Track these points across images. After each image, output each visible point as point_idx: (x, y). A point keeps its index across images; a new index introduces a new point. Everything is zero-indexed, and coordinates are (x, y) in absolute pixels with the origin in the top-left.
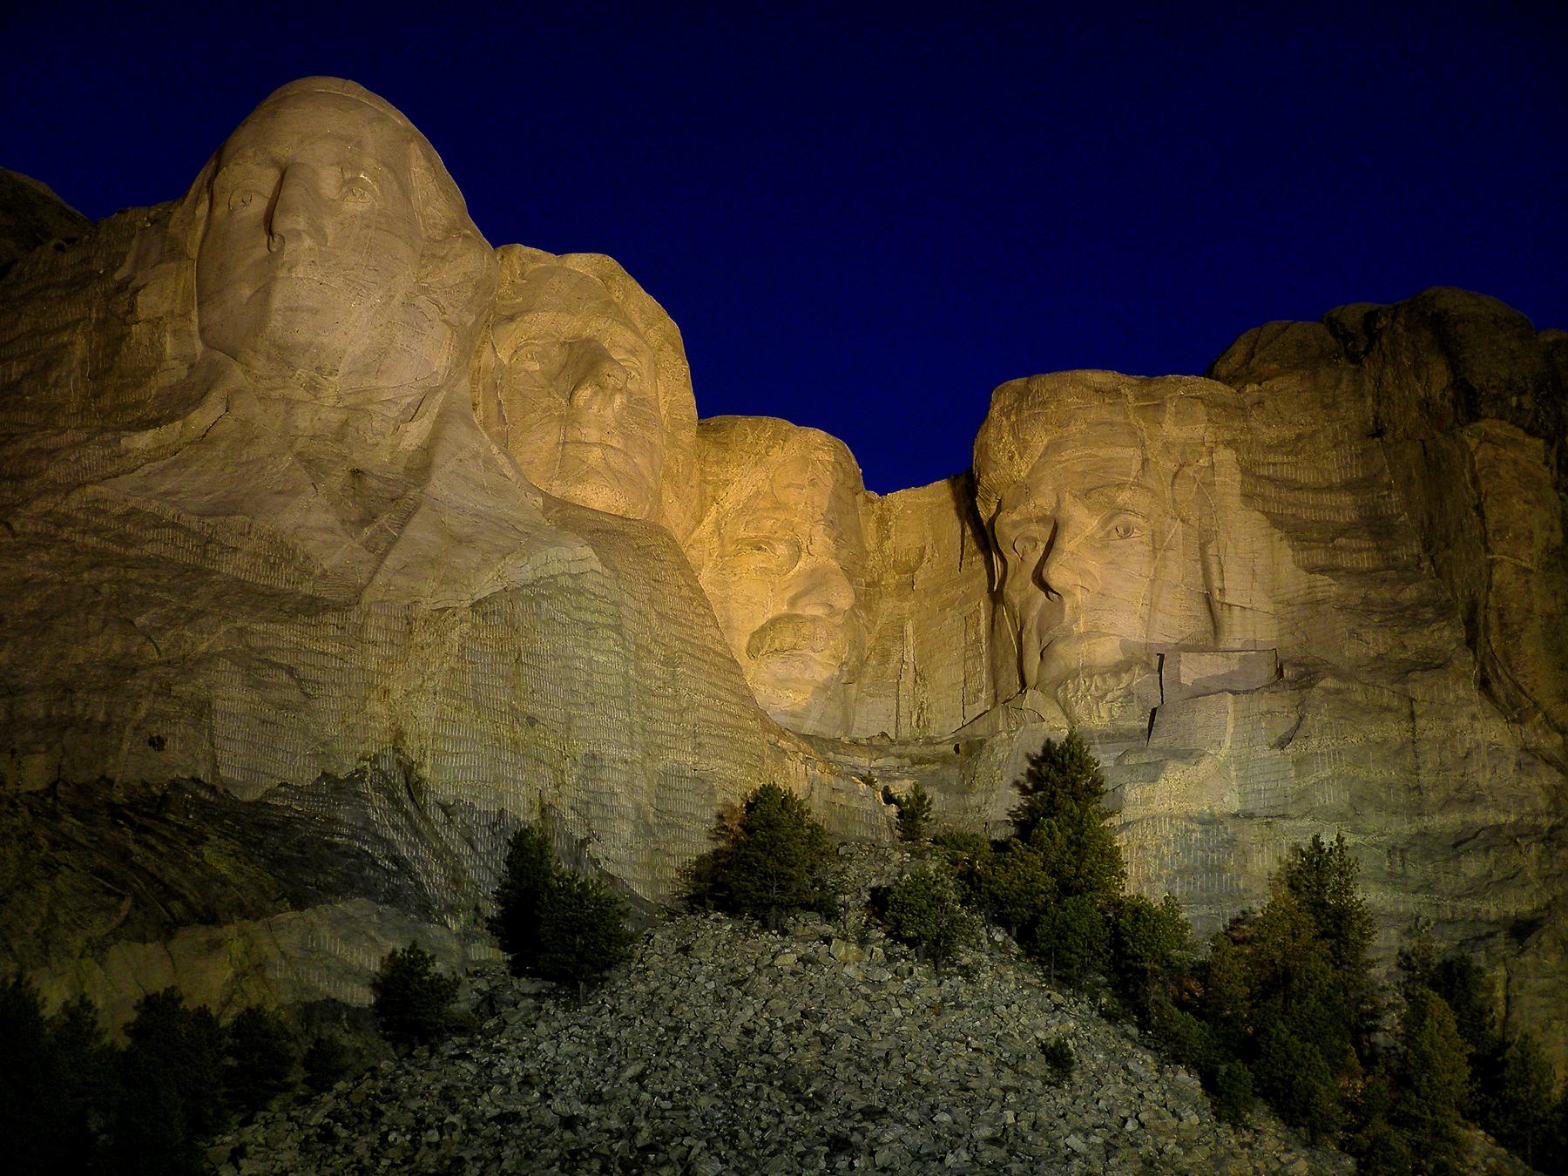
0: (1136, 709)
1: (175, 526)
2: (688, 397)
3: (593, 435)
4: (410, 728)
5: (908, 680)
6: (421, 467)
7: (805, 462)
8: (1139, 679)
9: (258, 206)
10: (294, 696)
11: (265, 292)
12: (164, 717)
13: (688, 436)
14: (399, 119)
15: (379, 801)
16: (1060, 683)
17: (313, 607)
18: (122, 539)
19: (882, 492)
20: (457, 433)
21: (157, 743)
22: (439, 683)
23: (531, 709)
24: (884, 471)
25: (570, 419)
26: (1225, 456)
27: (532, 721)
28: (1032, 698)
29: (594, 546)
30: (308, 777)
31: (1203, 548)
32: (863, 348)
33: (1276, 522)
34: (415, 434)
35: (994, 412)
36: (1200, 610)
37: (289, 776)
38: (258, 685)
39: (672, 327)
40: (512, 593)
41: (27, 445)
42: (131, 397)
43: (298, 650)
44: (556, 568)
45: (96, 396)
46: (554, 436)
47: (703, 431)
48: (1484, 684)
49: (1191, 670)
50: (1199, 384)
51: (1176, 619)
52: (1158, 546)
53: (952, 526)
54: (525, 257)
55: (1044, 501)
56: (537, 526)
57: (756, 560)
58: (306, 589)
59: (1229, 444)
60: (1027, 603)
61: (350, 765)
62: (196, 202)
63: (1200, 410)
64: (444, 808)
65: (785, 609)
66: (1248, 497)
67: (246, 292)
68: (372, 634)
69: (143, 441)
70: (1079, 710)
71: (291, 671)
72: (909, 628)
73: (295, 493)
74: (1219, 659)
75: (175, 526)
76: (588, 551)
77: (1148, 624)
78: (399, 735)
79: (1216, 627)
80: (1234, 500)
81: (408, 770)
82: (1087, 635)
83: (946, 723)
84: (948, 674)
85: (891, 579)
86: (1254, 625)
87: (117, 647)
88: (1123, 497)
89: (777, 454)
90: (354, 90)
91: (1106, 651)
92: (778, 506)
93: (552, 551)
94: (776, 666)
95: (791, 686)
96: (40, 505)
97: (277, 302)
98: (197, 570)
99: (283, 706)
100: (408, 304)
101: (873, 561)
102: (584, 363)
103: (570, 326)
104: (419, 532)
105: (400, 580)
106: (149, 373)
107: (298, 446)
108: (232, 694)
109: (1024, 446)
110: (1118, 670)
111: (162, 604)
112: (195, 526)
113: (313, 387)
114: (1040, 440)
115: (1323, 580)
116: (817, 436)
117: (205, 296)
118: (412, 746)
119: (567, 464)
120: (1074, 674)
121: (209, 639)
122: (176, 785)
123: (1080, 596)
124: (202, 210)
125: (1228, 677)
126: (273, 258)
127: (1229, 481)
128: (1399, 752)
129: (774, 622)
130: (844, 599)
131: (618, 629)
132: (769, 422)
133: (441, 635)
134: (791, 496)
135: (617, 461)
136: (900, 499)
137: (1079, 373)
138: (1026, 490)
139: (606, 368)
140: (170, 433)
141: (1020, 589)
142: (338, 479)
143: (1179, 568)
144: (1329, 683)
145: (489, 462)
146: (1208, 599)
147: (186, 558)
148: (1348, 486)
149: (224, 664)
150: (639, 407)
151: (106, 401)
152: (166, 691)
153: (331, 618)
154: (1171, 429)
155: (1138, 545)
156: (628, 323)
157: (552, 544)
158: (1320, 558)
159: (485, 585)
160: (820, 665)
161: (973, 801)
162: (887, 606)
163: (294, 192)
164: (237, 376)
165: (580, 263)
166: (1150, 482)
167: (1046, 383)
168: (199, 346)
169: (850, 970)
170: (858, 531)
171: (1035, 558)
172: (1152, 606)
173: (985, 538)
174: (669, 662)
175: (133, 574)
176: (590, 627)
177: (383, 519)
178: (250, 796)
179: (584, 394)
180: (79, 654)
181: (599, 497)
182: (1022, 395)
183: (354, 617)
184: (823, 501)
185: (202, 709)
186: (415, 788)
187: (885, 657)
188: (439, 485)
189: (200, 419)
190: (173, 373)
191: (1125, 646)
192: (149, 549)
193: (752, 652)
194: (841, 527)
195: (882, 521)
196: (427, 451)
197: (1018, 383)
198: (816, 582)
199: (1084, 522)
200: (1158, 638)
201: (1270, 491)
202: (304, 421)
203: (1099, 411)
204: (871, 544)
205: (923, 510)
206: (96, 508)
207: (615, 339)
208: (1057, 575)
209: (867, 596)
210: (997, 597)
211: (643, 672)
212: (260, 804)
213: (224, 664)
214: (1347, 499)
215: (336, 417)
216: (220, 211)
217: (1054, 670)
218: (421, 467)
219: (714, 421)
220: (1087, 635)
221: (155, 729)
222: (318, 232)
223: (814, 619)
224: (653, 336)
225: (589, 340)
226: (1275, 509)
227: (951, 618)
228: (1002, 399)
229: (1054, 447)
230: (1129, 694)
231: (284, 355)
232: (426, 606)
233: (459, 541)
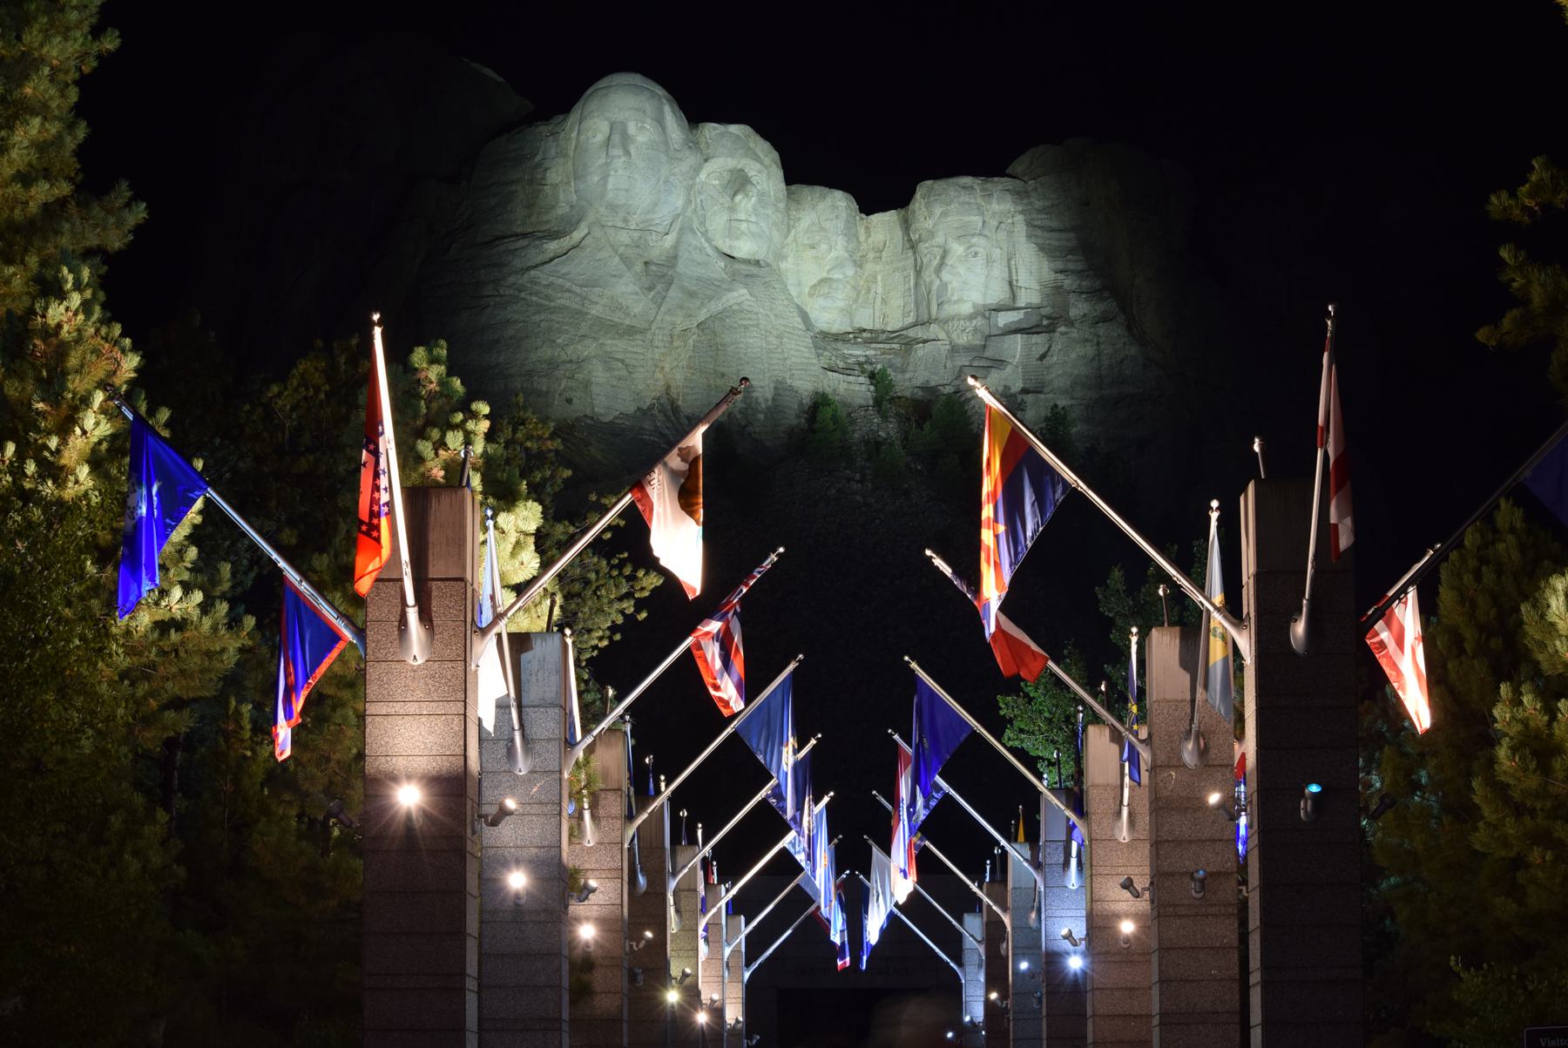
0: (979, 336)
1: (569, 291)
2: (779, 174)
3: (742, 216)
4: (673, 384)
5: (879, 301)
6: (673, 259)
7: (834, 207)
8: (979, 322)
9: (600, 138)
10: (625, 373)
11: (605, 178)
12: (571, 389)
13: (782, 205)
14: (660, 91)
15: (660, 417)
16: (946, 322)
17: (631, 331)
18: (547, 297)
19: (868, 214)
20: (689, 238)
21: (569, 401)
22: (685, 363)
23: (722, 370)
24: (869, 205)
25: (732, 209)
26: (1020, 218)
27: (723, 375)
28: (934, 328)
29: (746, 285)
30: (632, 409)
31: (1009, 260)
32: (861, 153)
33: (1042, 248)
34: (669, 240)
35: (918, 195)
36: (1007, 288)
37: (623, 410)
38: (611, 369)
39: (776, 155)
40: (713, 318)
41: (502, 248)
42: (545, 218)
43: (625, 351)
44: (732, 302)
45: (529, 216)
46: (725, 218)
47: (789, 194)
48: (1129, 328)
49: (1004, 319)
50: (1006, 182)
51: (998, 294)
52: (989, 261)
53: (899, 233)
54: (711, 130)
55: (939, 239)
56: (722, 281)
57: (810, 253)
58: (627, 322)
59: (1021, 212)
60: (931, 283)
61: (648, 402)
62: (571, 130)
63: (1008, 196)
64: (688, 418)
65: (825, 275)
66: (1029, 237)
67: (596, 178)
68: (656, 343)
69: (553, 246)
70: (954, 336)
71: (622, 361)
72: (879, 278)
73: (620, 277)
74: (1014, 313)
75: (569, 291)
76: (744, 291)
77: (985, 295)
78: (668, 387)
79: (1014, 297)
80: (1023, 239)
81: (672, 402)
82: (956, 302)
83: (894, 324)
84: (897, 302)
85: (871, 255)
86: (1030, 295)
87: (549, 352)
88: (975, 240)
89: (821, 206)
90: (637, 79)
91: (966, 309)
92: (823, 229)
93: (731, 295)
94: (821, 302)
95: (829, 315)
96: (511, 280)
97: (610, 186)
98: (579, 312)
99: (620, 379)
100: (666, 182)
101: (864, 246)
102: (739, 183)
103: (732, 163)
104: (673, 293)
105: (668, 318)
106: (553, 207)
107: (621, 250)
108: (598, 374)
109: (931, 214)
110: (971, 317)
111: (567, 332)
112: (578, 290)
113: (626, 220)
114: (938, 211)
115: (1061, 276)
116: (839, 194)
117: (577, 176)
118: (674, 392)
119: (731, 232)
120: (952, 318)
121: (588, 349)
122: (577, 419)
123: (955, 284)
124: (574, 135)
125: (1019, 321)
126: (607, 164)
127: (1021, 229)
128: (1093, 359)
129: (823, 281)
130: (850, 271)
131: (757, 326)
132: (819, 190)
133: (686, 342)
134: (827, 225)
135: (753, 228)
136: (877, 218)
137: (955, 180)
138: (932, 234)
139: (749, 187)
140: (565, 243)
141: (928, 275)
142: (639, 267)
143: (999, 271)
144: (1062, 329)
145: (701, 250)
146: (1010, 283)
147: (575, 306)
148: (1073, 229)
149: (595, 361)
150: (762, 195)
151: (534, 218)
152: (572, 378)
153: (639, 337)
154: (995, 206)
155: (980, 260)
156: (757, 159)
157: (730, 290)
158: (1060, 265)
159: (702, 315)
160: (841, 297)
161: (908, 376)
162: (869, 267)
163: (616, 138)
164: (591, 217)
165: (734, 129)
166: (986, 232)
167: (939, 185)
168: (575, 197)
169: (858, 498)
170: (856, 236)
171: (935, 262)
172: (986, 287)
173: (913, 246)
174: (778, 337)
175: (554, 317)
176: (746, 327)
177: (659, 287)
178: (608, 419)
179: (739, 197)
180: (533, 357)
181: (744, 248)
182: (931, 189)
183: (649, 336)
184: (841, 225)
185: (587, 384)
186: (676, 409)
187: (869, 290)
188: (681, 267)
189: (577, 235)
190: (562, 209)
191: (974, 306)
192: (562, 301)
193: (811, 295)
194: (850, 234)
195: (867, 228)
196: (676, 247)
197: (929, 182)
198: (839, 265)
199: (958, 249)
200: (989, 301)
201: (1039, 232)
202: (624, 237)
203: (965, 198)
204: (862, 238)
205: (884, 223)
206: (533, 282)
207: (752, 169)
208: (945, 276)
209: (859, 264)
210: (918, 273)
211: (768, 343)
212: (612, 422)
213: (595, 361)
214: (1072, 235)
215: (636, 235)
216: (582, 138)
217: (943, 315)
218: (673, 259)
219: (793, 187)
220: (956, 302)
221: (568, 394)
222: (627, 153)
223: (838, 280)
224: (767, 161)
225: (742, 170)
226: (1040, 241)
227: (898, 276)
228: (922, 189)
229: (944, 214)
230: (976, 330)
231: (613, 208)
232: (677, 331)
233: (692, 295)
